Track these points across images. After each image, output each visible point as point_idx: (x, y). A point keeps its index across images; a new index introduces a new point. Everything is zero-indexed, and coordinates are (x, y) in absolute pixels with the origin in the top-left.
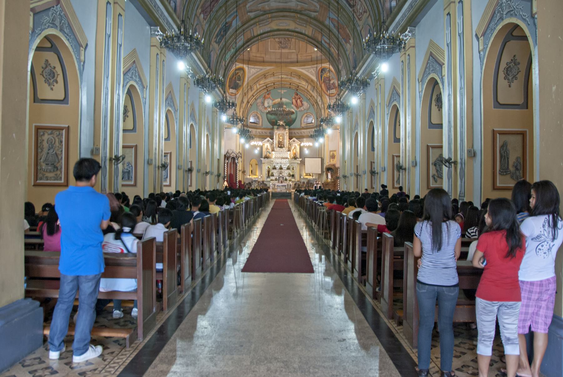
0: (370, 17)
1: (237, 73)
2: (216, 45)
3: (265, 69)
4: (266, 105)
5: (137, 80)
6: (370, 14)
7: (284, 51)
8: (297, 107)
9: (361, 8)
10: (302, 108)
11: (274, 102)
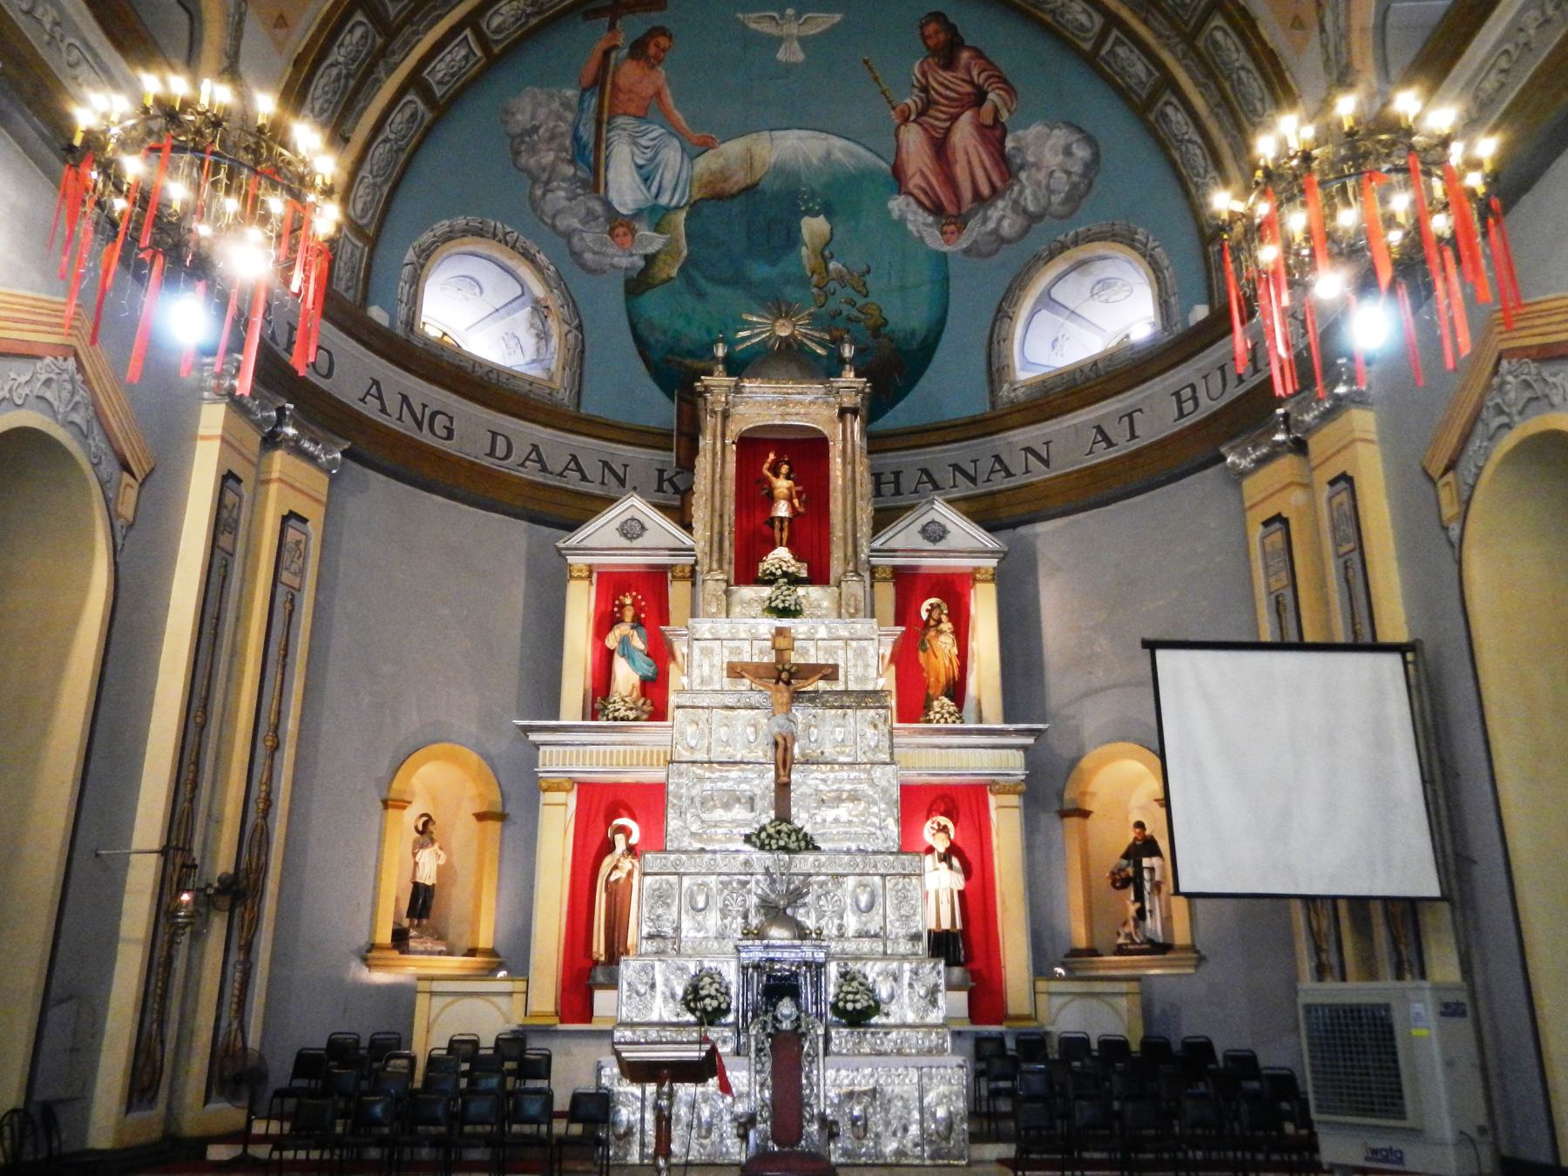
4: (625, 190)
8: (943, 212)
10: (1001, 217)
11: (706, 163)
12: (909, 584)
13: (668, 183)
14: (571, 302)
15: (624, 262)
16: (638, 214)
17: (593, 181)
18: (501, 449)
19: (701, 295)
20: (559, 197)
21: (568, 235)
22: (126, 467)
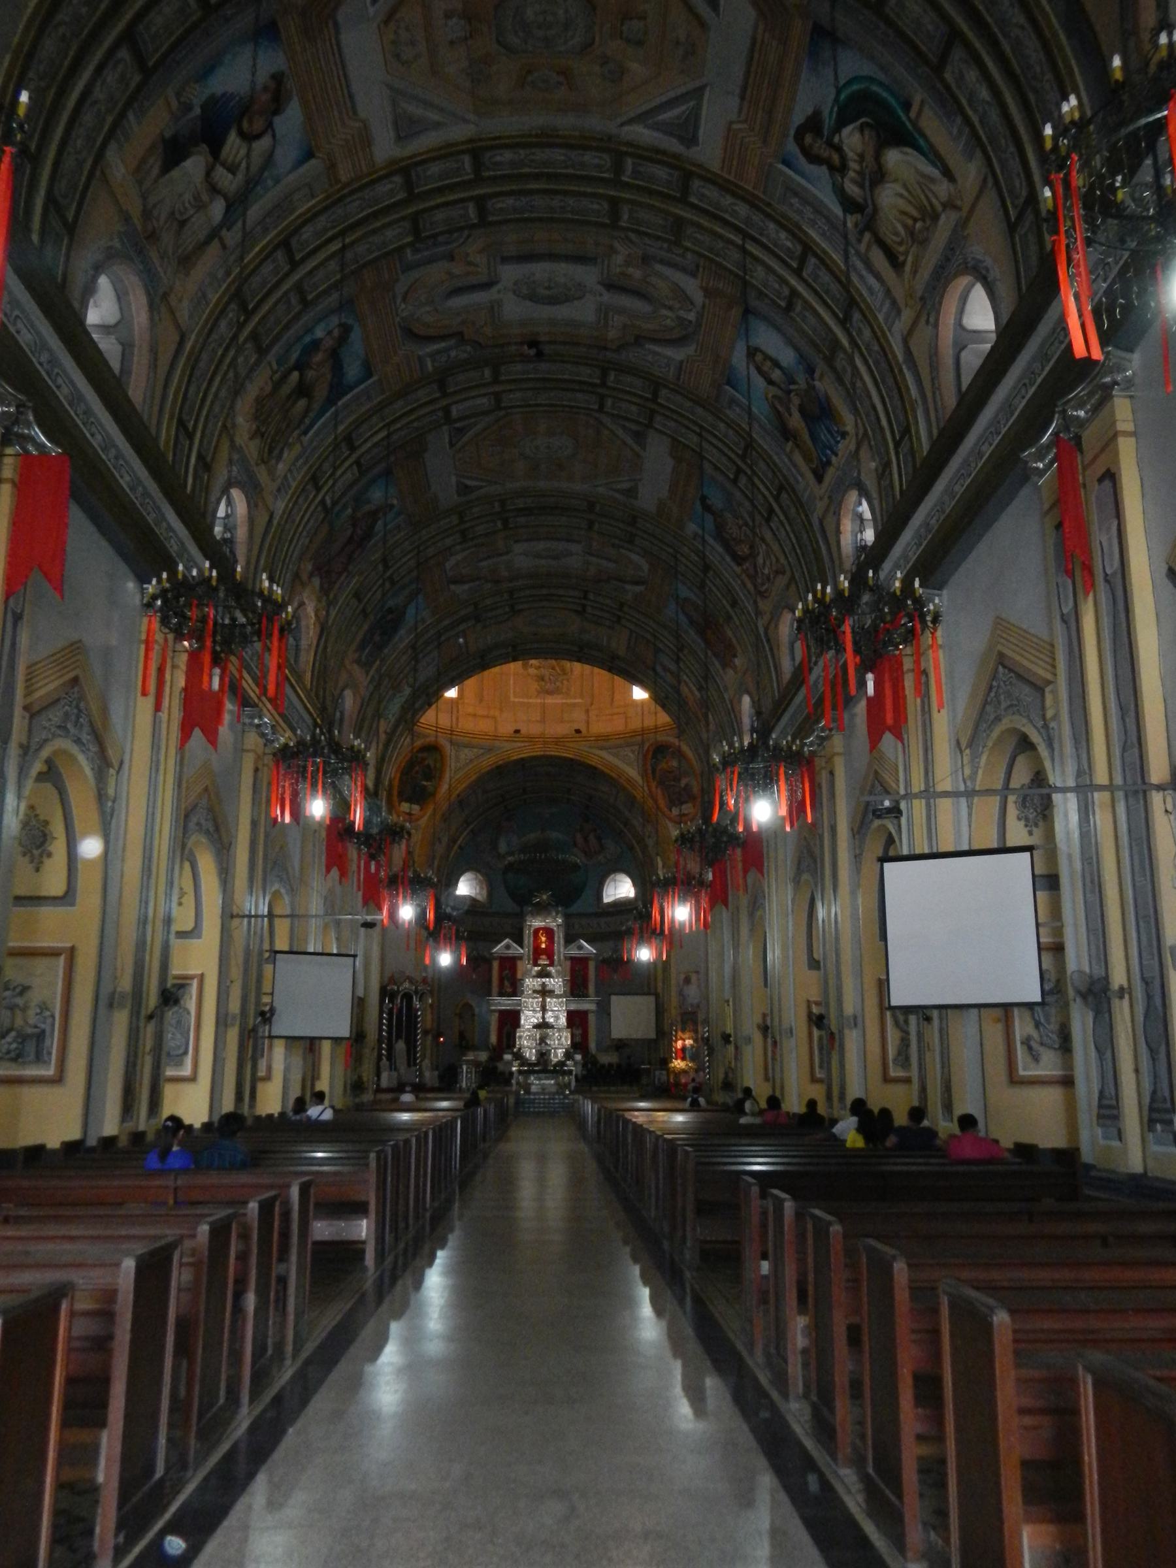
0: (793, 586)
1: (423, 759)
2: (357, 671)
4: (503, 847)
5: (85, 737)
6: (793, 578)
7: (550, 700)
9: (768, 563)
10: (601, 857)
12: (573, 960)
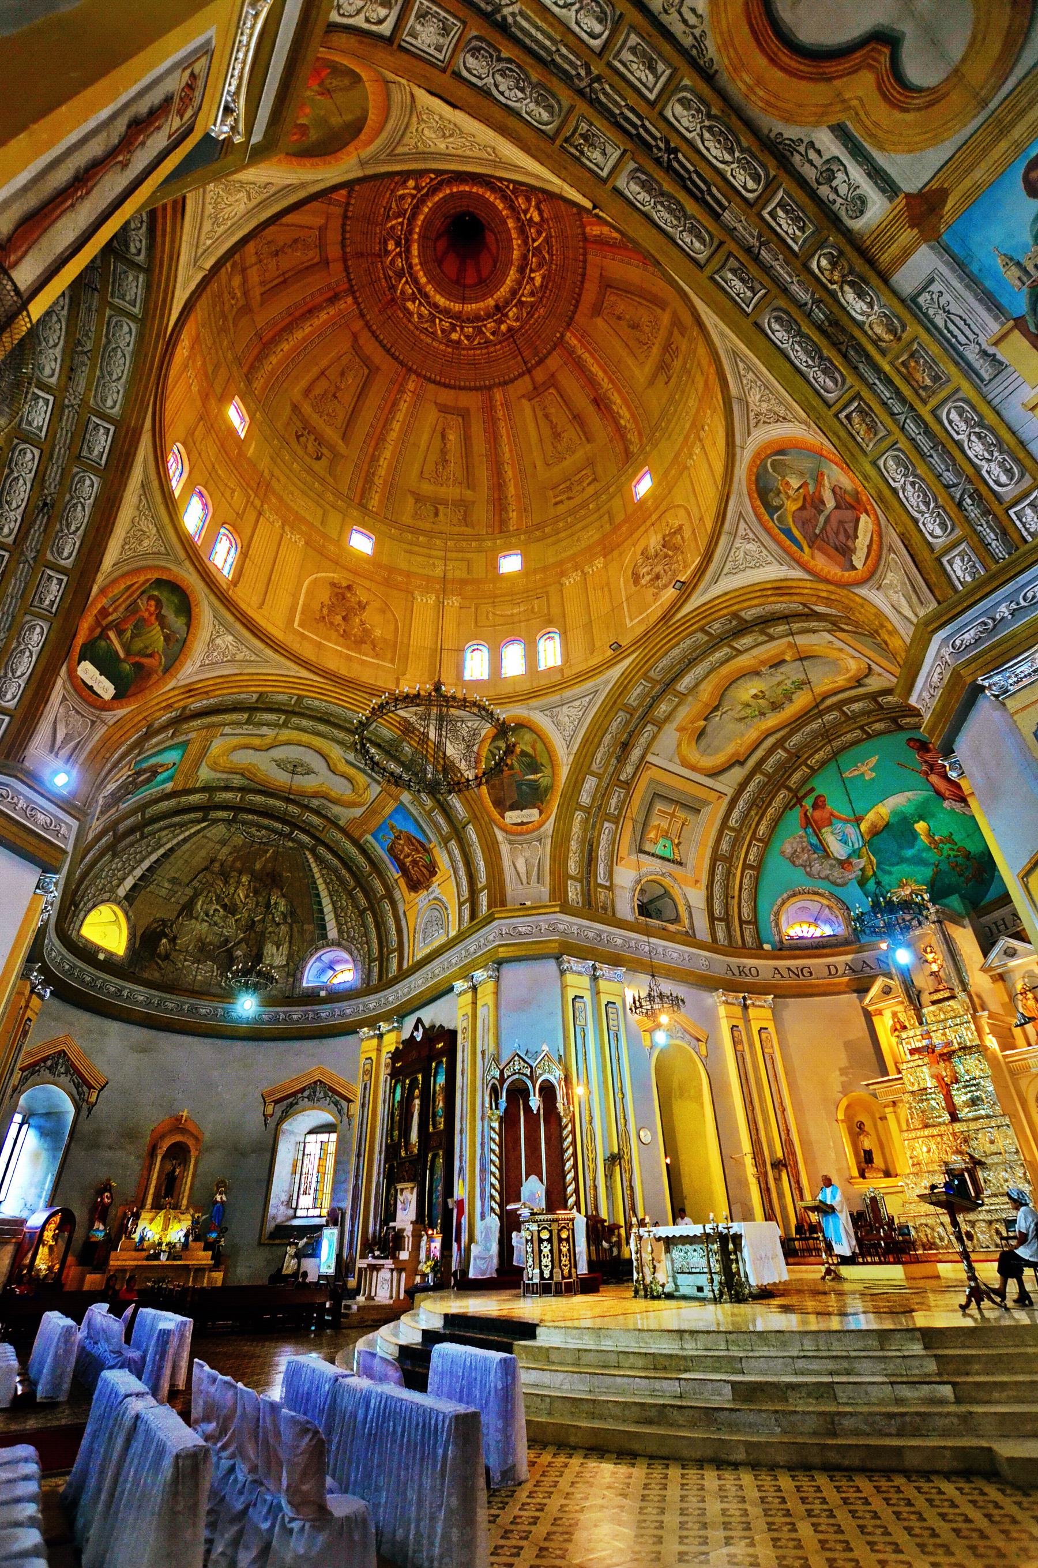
3: (608, 682)
4: (838, 849)
11: (864, 826)
13: (854, 839)
14: (839, 900)
15: (853, 875)
16: (850, 856)
17: (826, 854)
18: (833, 971)
19: (890, 873)
20: (817, 867)
21: (827, 878)
22: (699, 1040)
